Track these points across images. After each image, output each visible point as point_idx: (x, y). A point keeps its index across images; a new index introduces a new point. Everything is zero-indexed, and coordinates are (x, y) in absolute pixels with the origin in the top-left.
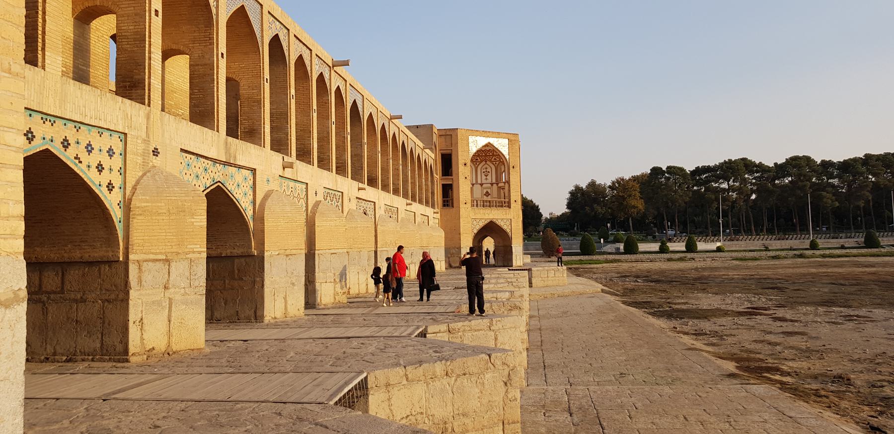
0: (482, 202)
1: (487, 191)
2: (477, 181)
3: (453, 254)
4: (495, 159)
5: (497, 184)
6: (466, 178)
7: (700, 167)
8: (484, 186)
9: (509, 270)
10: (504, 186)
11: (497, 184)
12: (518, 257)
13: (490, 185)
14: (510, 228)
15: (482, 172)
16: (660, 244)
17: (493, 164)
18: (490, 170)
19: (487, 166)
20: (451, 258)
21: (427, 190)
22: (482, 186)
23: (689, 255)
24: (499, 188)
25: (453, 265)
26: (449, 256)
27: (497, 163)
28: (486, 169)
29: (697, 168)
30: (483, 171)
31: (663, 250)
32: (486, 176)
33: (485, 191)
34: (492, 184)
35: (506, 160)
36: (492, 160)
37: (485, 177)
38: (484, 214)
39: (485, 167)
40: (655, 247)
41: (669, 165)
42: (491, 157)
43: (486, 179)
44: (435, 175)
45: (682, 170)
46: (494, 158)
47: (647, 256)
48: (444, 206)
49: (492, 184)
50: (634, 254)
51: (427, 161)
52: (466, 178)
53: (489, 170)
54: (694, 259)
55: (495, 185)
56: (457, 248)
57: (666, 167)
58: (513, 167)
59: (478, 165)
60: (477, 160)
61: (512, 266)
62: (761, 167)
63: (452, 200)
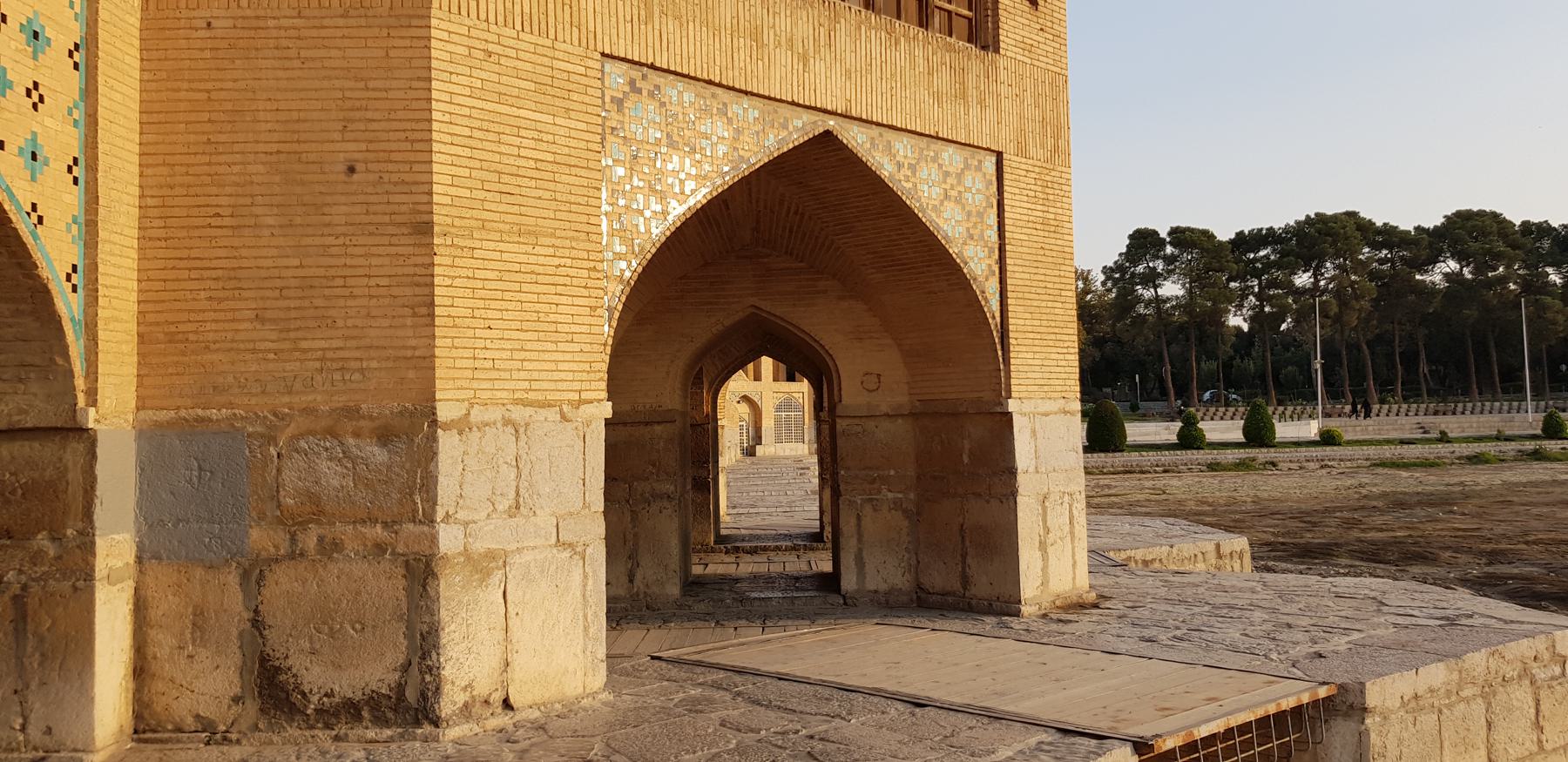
3: (315, 509)
7: (1247, 233)
12: (1058, 519)
16: (1180, 424)
20: (282, 583)
23: (1262, 454)
26: (262, 538)
29: (1240, 234)
31: (1190, 439)
38: (756, 36)
40: (1167, 431)
41: (1174, 225)
45: (1207, 235)
47: (1152, 456)
50: (1114, 451)
54: (1274, 464)
56: (385, 436)
57: (1169, 229)
62: (1388, 237)
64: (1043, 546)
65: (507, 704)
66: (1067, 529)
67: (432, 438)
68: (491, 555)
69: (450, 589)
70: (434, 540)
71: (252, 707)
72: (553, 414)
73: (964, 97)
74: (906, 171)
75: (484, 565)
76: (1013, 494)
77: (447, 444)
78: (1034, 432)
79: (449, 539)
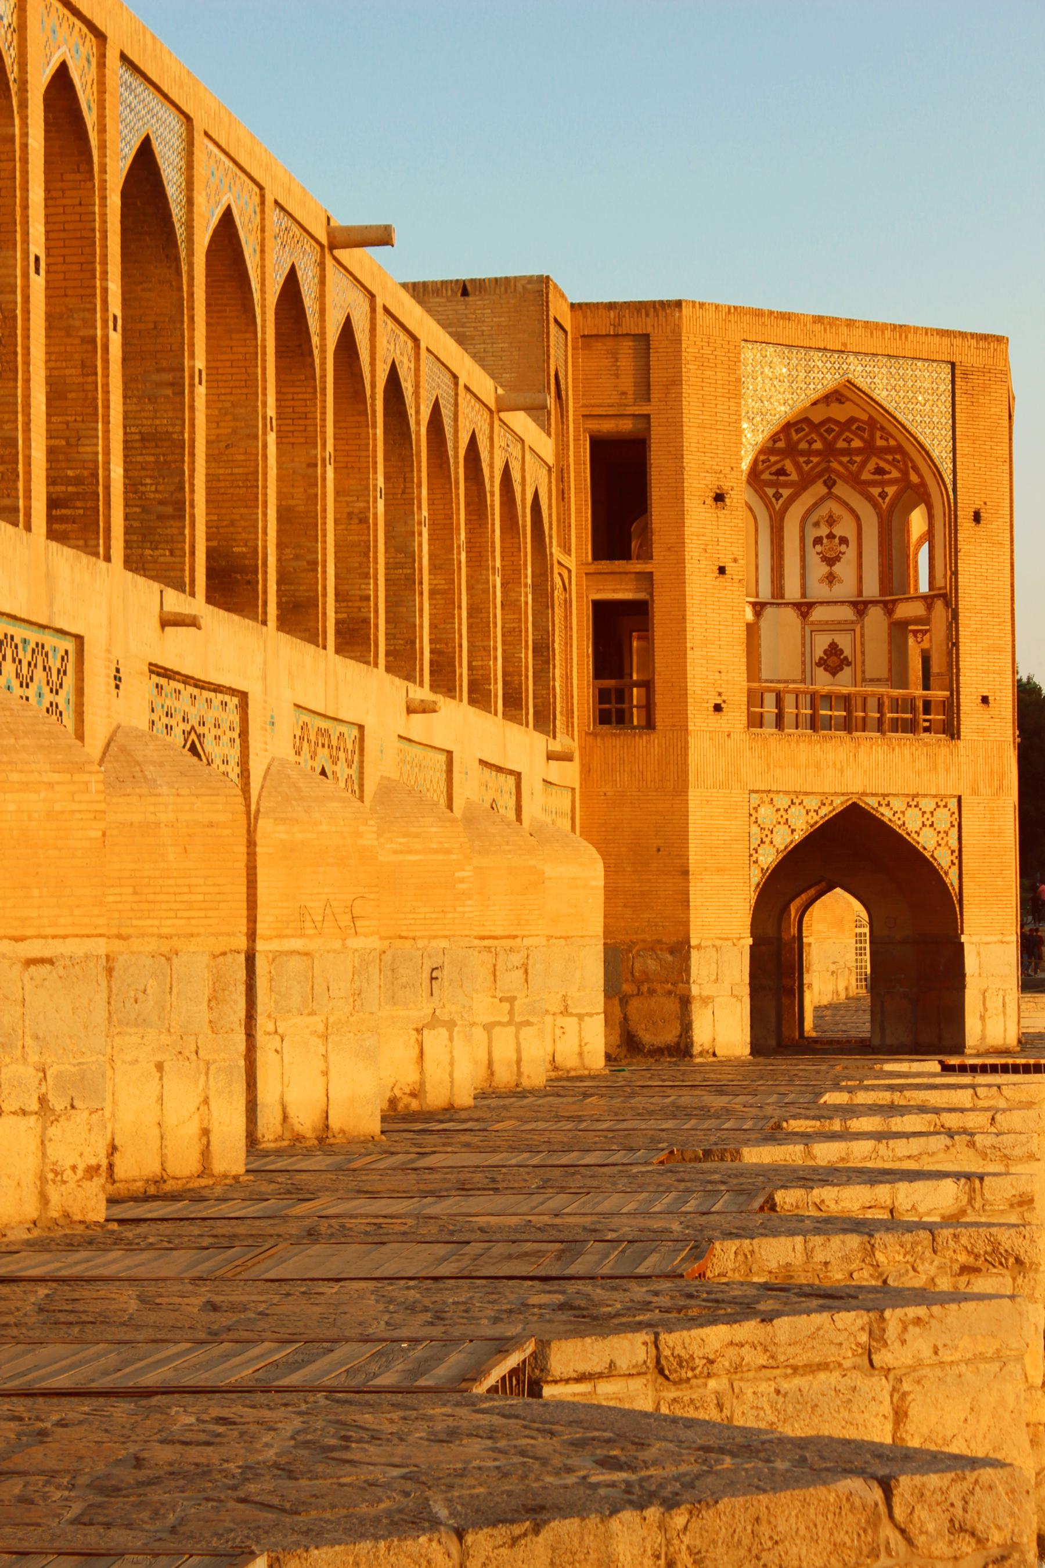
0: (803, 699)
1: (833, 645)
2: (778, 589)
3: (646, 978)
4: (879, 471)
5: (888, 608)
6: (722, 570)
8: (818, 614)
9: (947, 1068)
10: (926, 621)
11: (888, 608)
13: (847, 613)
14: (954, 844)
15: (809, 542)
17: (869, 498)
18: (850, 533)
19: (832, 507)
20: (635, 1004)
21: (512, 636)
22: (804, 616)
24: (899, 629)
25: (648, 1038)
26: (627, 988)
27: (891, 490)
28: (831, 521)
30: (812, 533)
32: (831, 561)
33: (822, 643)
34: (860, 607)
35: (938, 474)
36: (866, 476)
37: (824, 569)
39: (823, 511)
42: (858, 459)
43: (831, 579)
44: (556, 551)
46: (871, 466)
48: (603, 718)
49: (860, 607)
51: (516, 475)
52: (722, 570)
53: (845, 528)
55: (875, 614)
58: (977, 517)
59: (791, 500)
60: (782, 472)
61: (959, 1048)
63: (648, 685)
64: (982, 1018)
65: (714, 1055)
66: (1001, 1009)
67: (689, 952)
68: (708, 997)
69: (696, 1008)
70: (690, 990)
71: (624, 1049)
72: (730, 943)
73: (935, 769)
74: (897, 815)
75: (706, 1000)
76: (964, 987)
77: (694, 953)
78: (979, 954)
79: (695, 990)
